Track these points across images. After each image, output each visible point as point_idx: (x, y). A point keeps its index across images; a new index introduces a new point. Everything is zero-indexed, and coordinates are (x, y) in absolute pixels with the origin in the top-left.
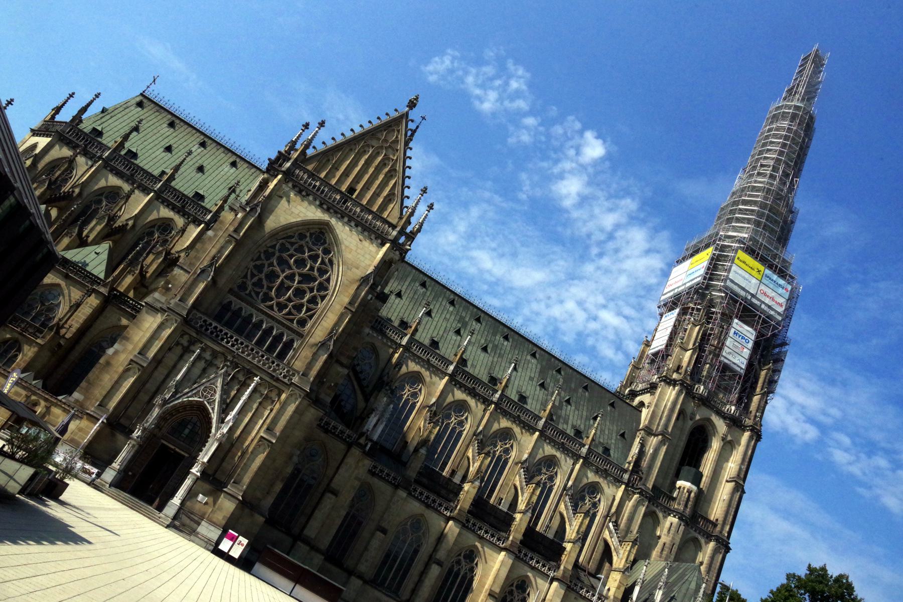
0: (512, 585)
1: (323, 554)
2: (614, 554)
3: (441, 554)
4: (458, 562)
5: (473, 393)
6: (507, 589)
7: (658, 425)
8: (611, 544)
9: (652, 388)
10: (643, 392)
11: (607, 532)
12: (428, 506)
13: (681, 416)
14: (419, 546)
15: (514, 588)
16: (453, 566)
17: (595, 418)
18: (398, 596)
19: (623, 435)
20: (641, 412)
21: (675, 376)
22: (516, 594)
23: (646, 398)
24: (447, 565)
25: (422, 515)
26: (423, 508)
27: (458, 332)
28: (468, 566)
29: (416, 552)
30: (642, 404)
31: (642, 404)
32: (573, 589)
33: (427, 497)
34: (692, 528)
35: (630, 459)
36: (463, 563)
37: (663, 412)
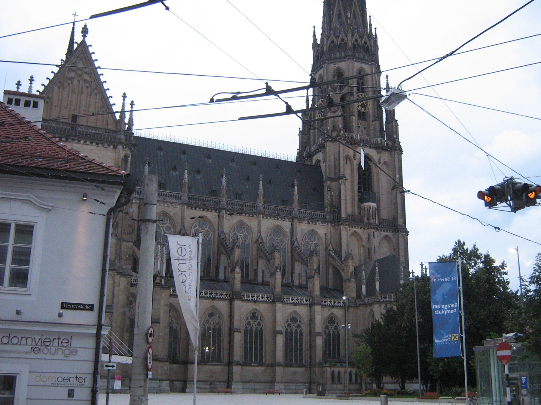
0: (288, 321)
1: (167, 361)
2: (341, 271)
3: (236, 324)
4: (249, 323)
5: (205, 208)
6: (286, 325)
7: (335, 173)
8: (336, 265)
9: (322, 147)
10: (317, 152)
11: (331, 259)
12: (214, 299)
13: (348, 160)
14: (220, 326)
15: (290, 322)
16: (246, 327)
17: (294, 187)
18: (220, 362)
19: (315, 189)
20: (320, 166)
21: (335, 134)
22: (292, 325)
23: (319, 156)
24: (243, 329)
25: (213, 306)
26: (210, 301)
27: (175, 169)
28: (256, 323)
29: (220, 330)
30: (318, 161)
31: (318, 161)
32: (325, 306)
33: (211, 294)
34: (381, 230)
35: (326, 204)
36: (252, 323)
37: (335, 164)
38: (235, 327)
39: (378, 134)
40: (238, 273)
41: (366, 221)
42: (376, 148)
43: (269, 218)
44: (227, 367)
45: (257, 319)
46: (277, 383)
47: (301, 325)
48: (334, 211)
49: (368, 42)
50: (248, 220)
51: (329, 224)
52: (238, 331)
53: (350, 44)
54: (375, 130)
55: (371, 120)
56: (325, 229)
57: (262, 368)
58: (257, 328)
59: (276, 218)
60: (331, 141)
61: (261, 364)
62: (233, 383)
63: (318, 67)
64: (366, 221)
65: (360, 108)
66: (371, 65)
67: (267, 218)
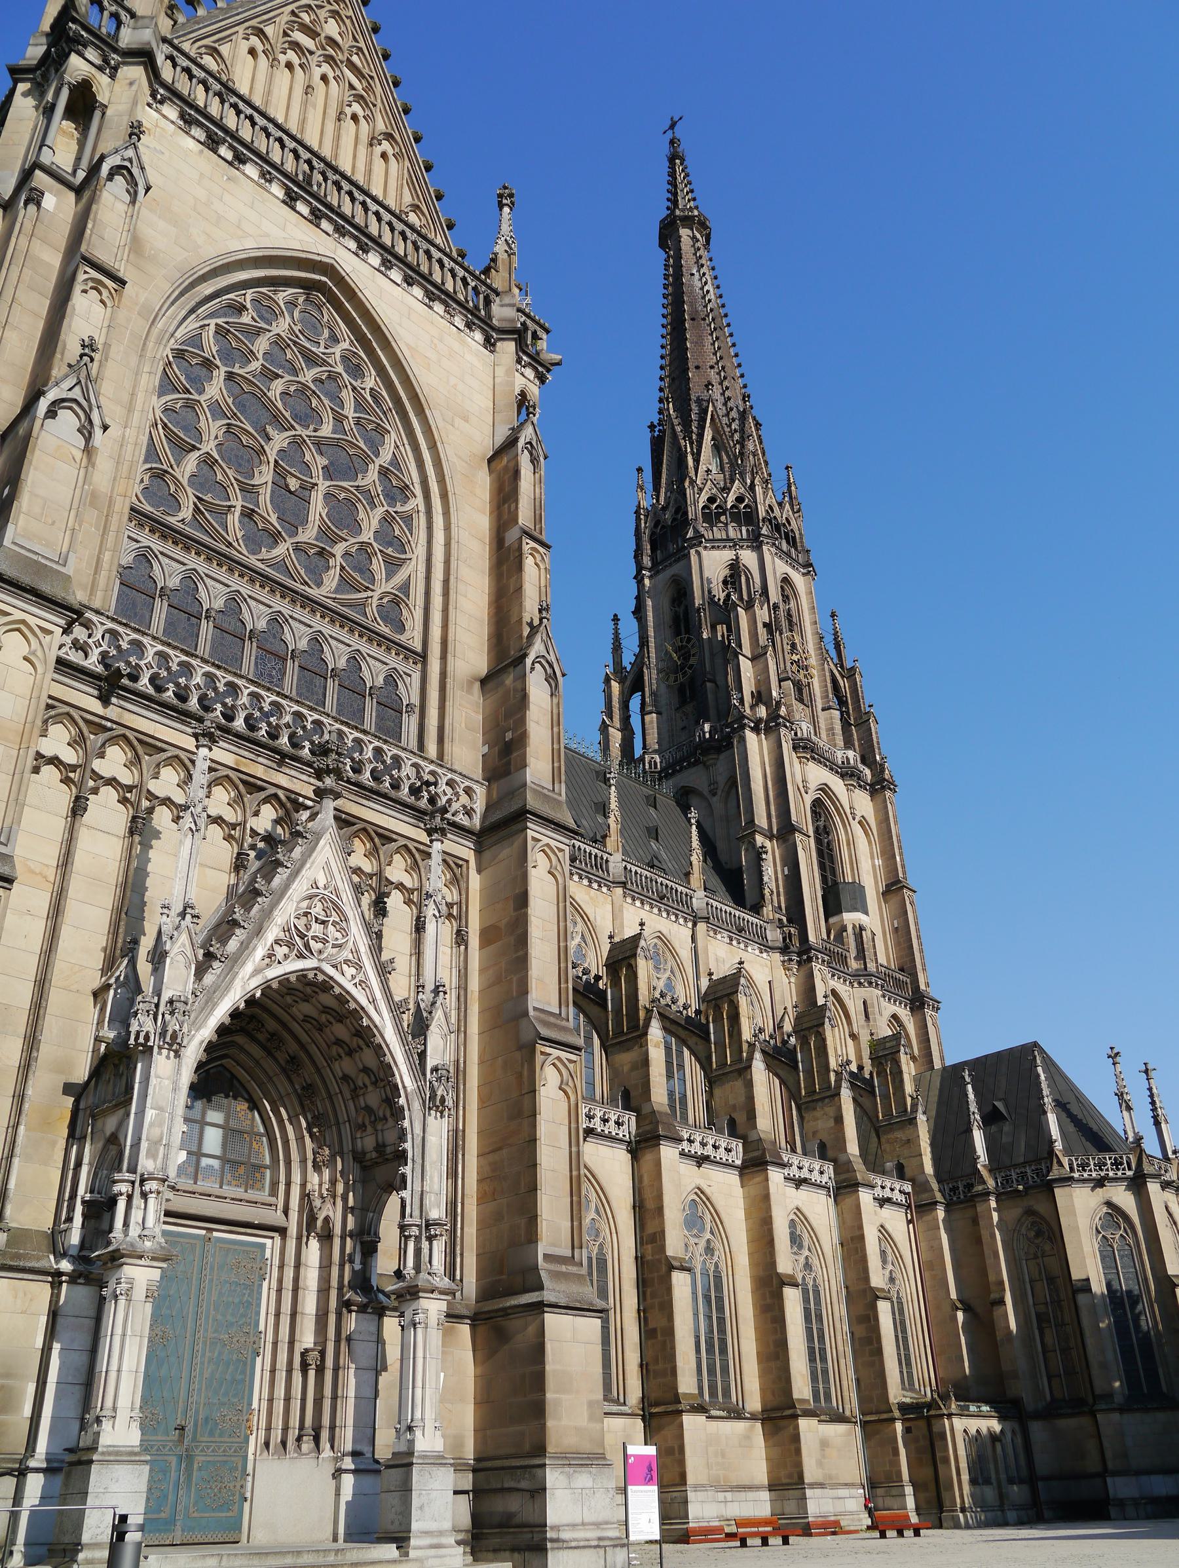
18: (617, 1402)
38: (670, 1252)
39: (840, 741)
40: (657, 1046)
41: (854, 965)
42: (843, 776)
43: (638, 903)
44: (639, 1424)
45: (702, 1229)
46: (813, 1486)
47: (815, 1262)
48: (780, 920)
49: (793, 522)
50: (587, 897)
51: (777, 957)
52: (683, 1269)
53: (762, 513)
54: (831, 730)
55: (820, 707)
56: (767, 970)
57: (740, 1426)
58: (704, 1262)
59: (655, 910)
60: (752, 729)
61: (736, 1414)
62: (691, 1495)
63: (663, 561)
64: (854, 965)
65: (795, 667)
66: (804, 574)
67: (633, 904)
